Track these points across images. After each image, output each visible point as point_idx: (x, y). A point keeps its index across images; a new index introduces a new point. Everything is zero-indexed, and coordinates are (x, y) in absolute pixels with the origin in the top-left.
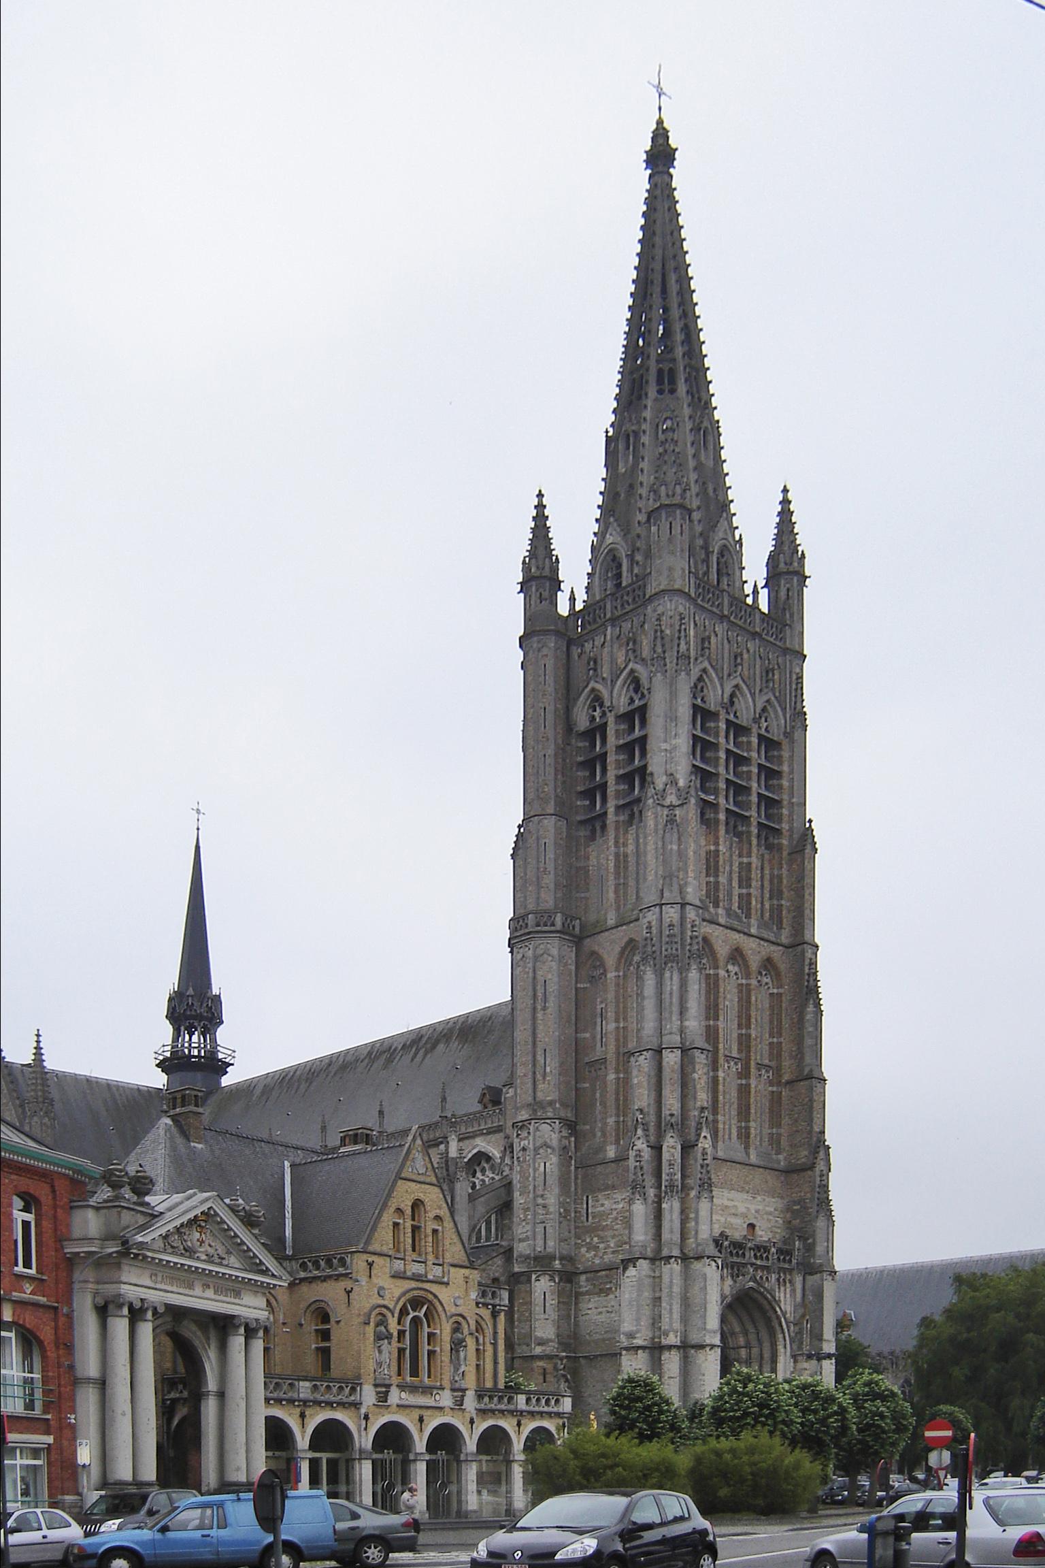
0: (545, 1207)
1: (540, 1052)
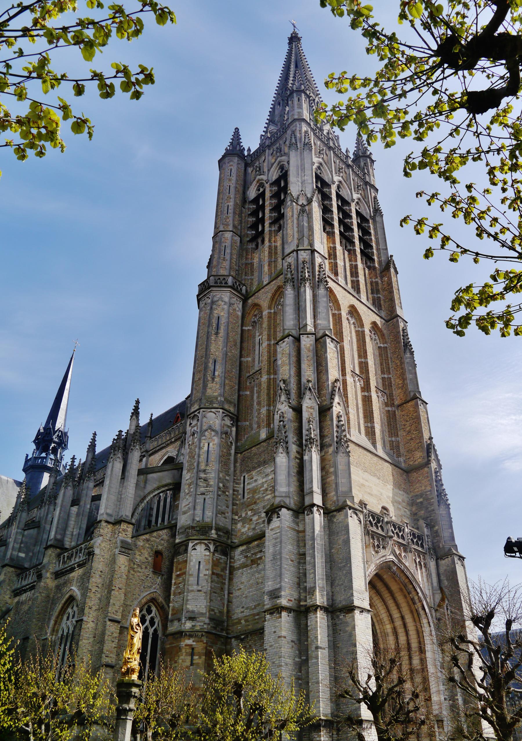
0: (205, 480)
1: (211, 361)
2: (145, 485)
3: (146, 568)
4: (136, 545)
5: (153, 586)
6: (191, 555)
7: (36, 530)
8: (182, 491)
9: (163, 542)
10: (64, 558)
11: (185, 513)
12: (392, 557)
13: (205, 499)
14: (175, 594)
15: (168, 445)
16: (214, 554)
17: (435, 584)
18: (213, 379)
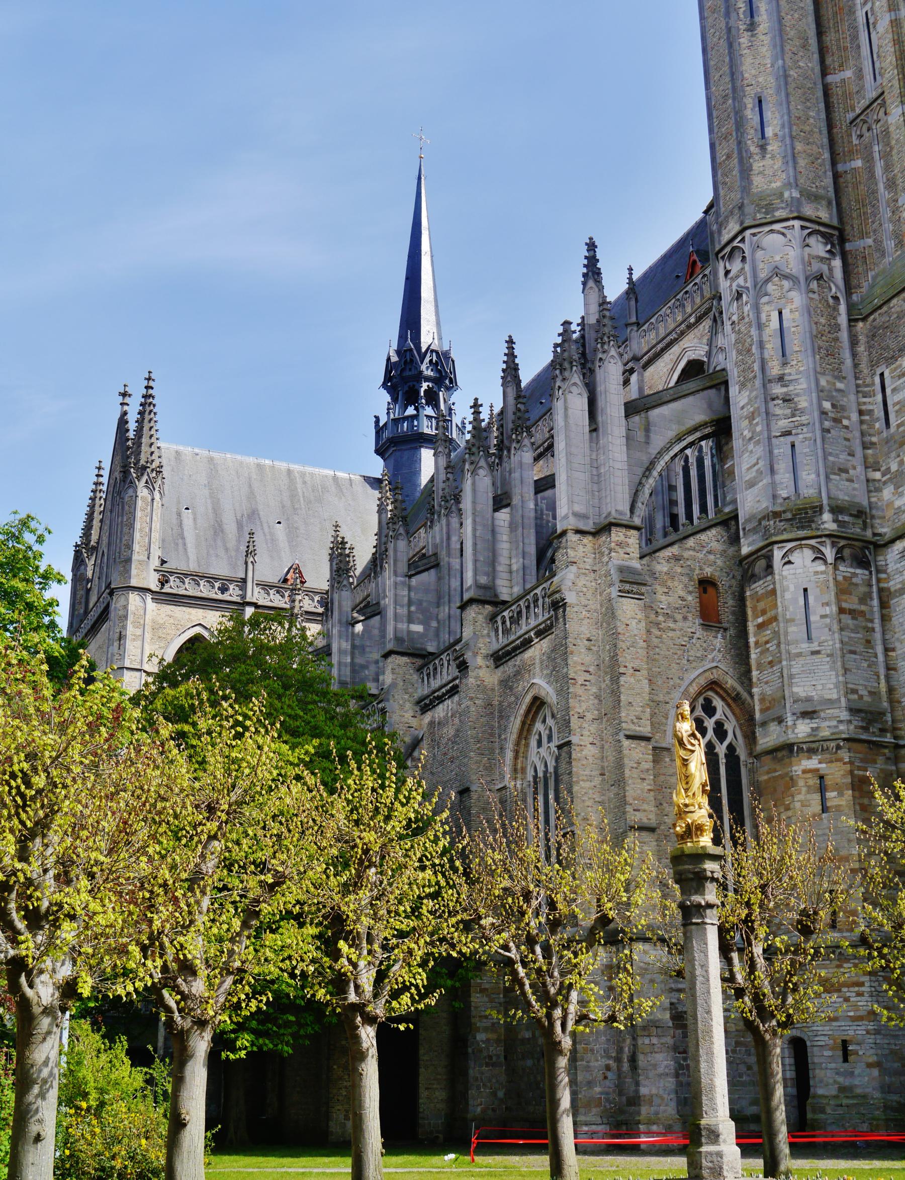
0: (787, 400)
1: (750, 103)
2: (648, 437)
3: (685, 618)
4: (653, 574)
5: (711, 655)
6: (784, 578)
7: (433, 571)
8: (735, 434)
9: (712, 557)
10: (504, 622)
11: (751, 484)
13: (793, 446)
14: (760, 667)
15: (682, 334)
16: (836, 568)
18: (763, 148)
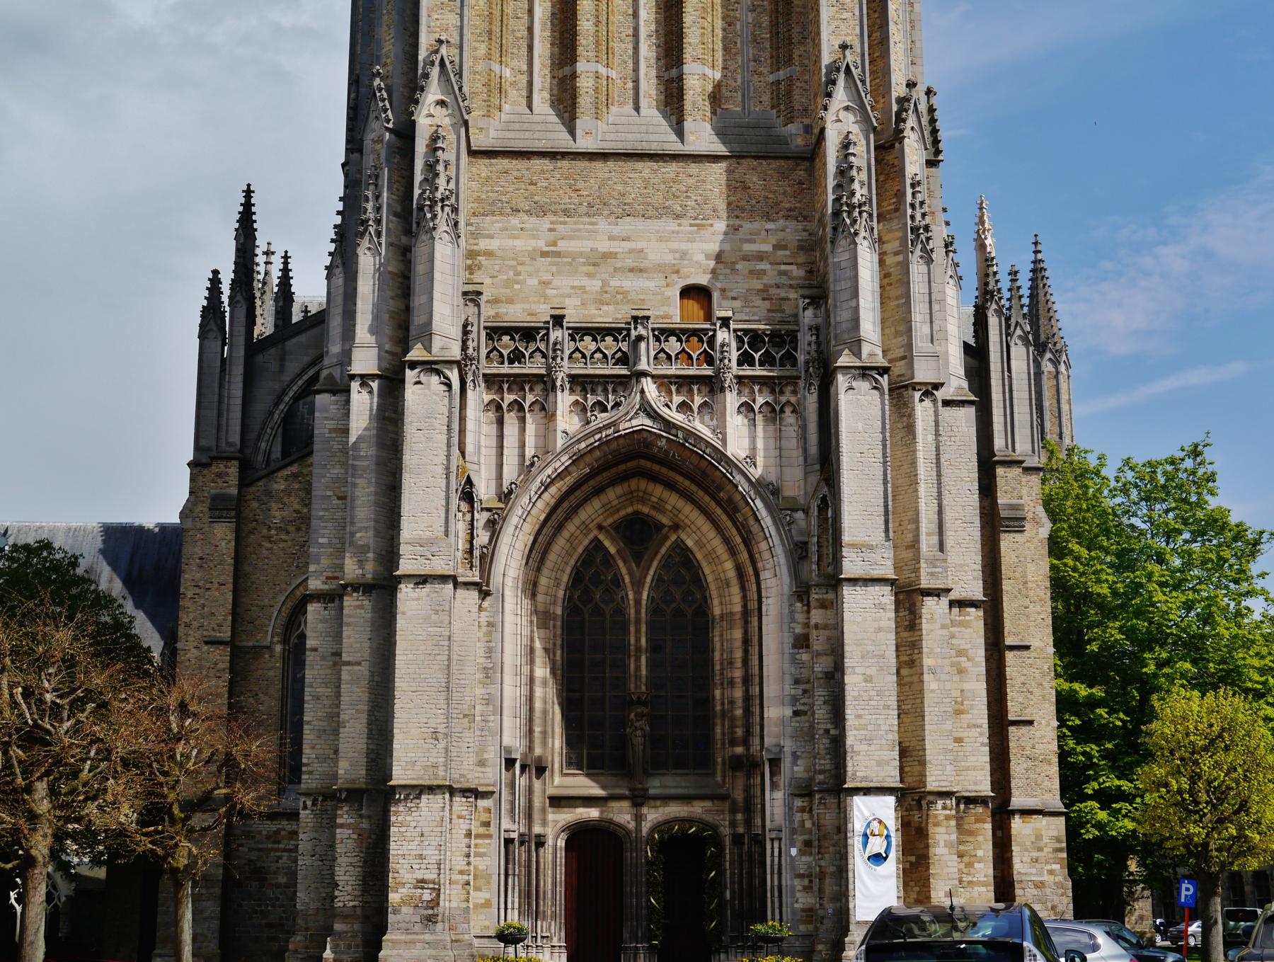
2: (282, 366)
12: (643, 421)
17: (813, 449)
